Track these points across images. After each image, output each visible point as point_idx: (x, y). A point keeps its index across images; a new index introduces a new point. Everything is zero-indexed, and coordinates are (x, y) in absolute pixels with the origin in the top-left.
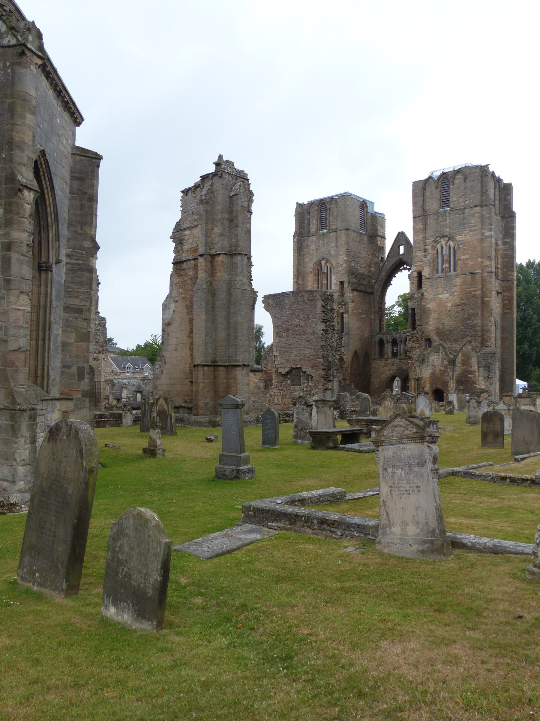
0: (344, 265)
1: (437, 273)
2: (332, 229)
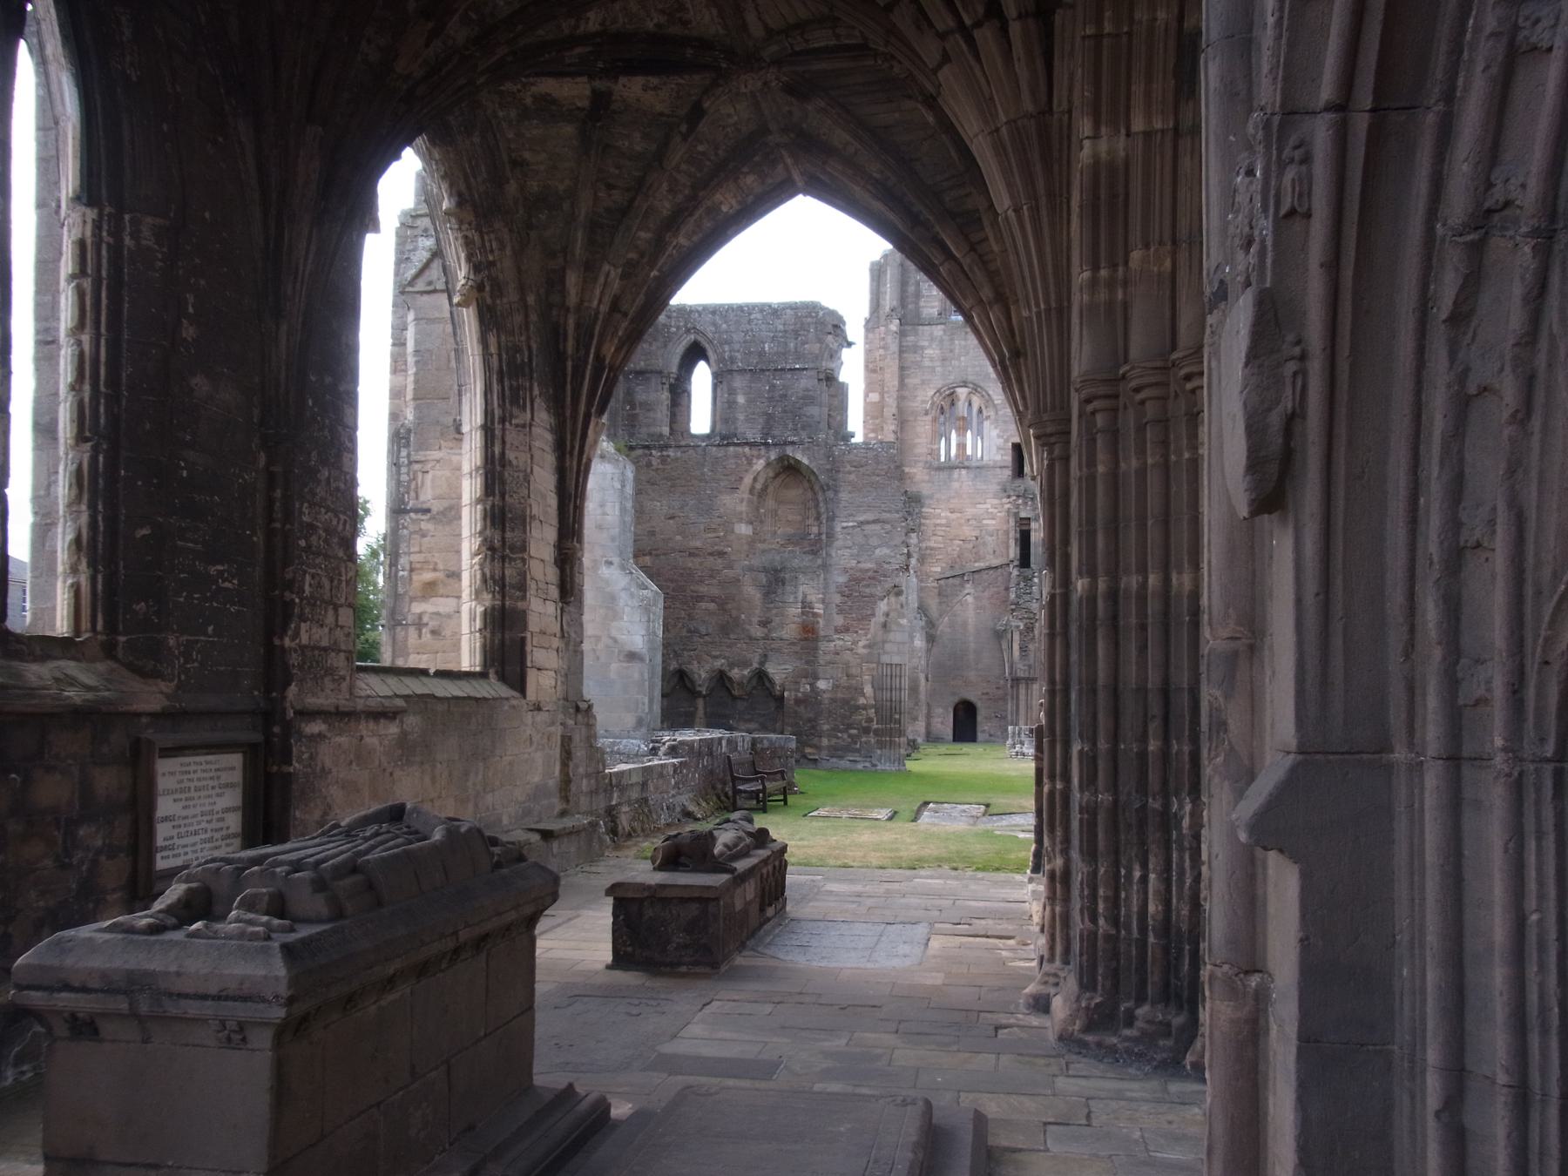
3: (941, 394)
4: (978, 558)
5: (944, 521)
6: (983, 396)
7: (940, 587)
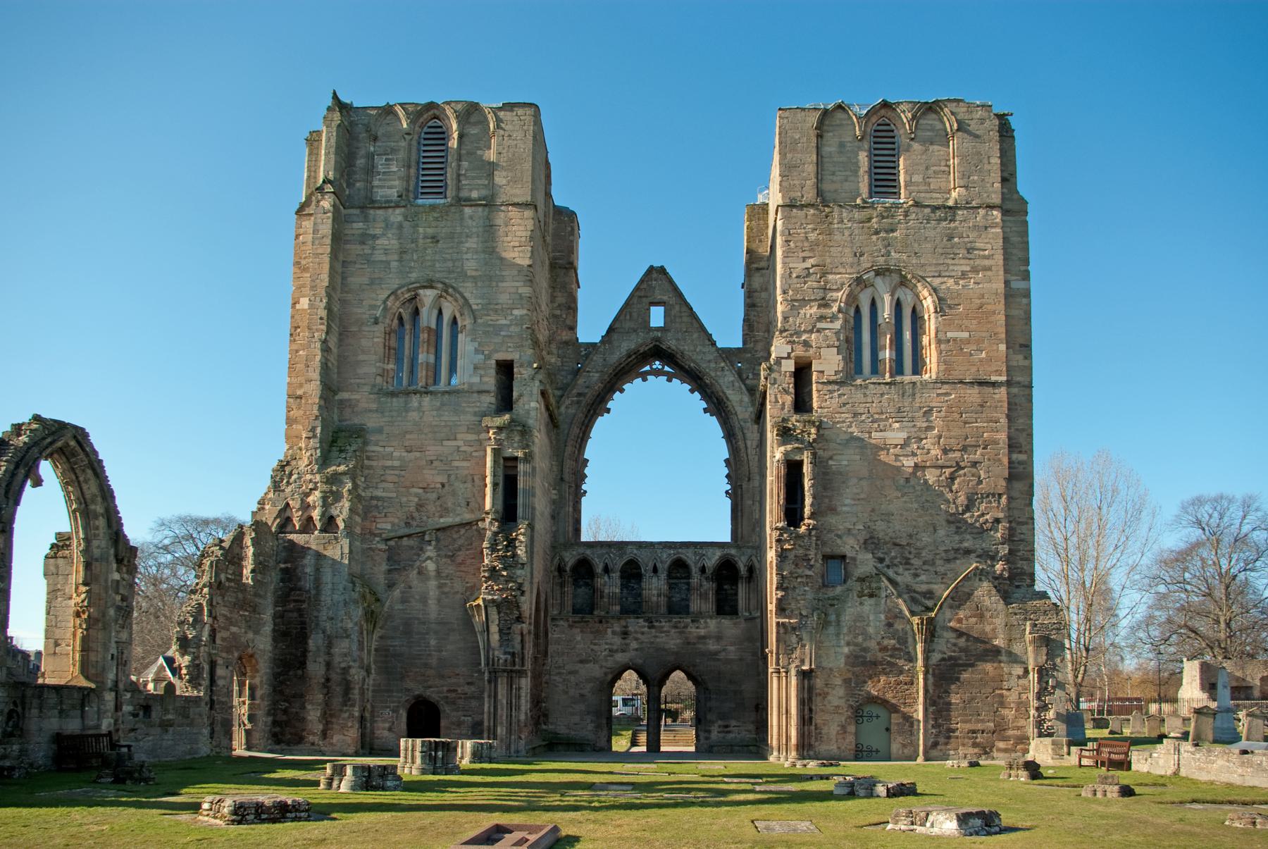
0: (516, 312)
2: (468, 199)
3: (397, 298)
4: (445, 511)
5: (396, 463)
7: (390, 548)
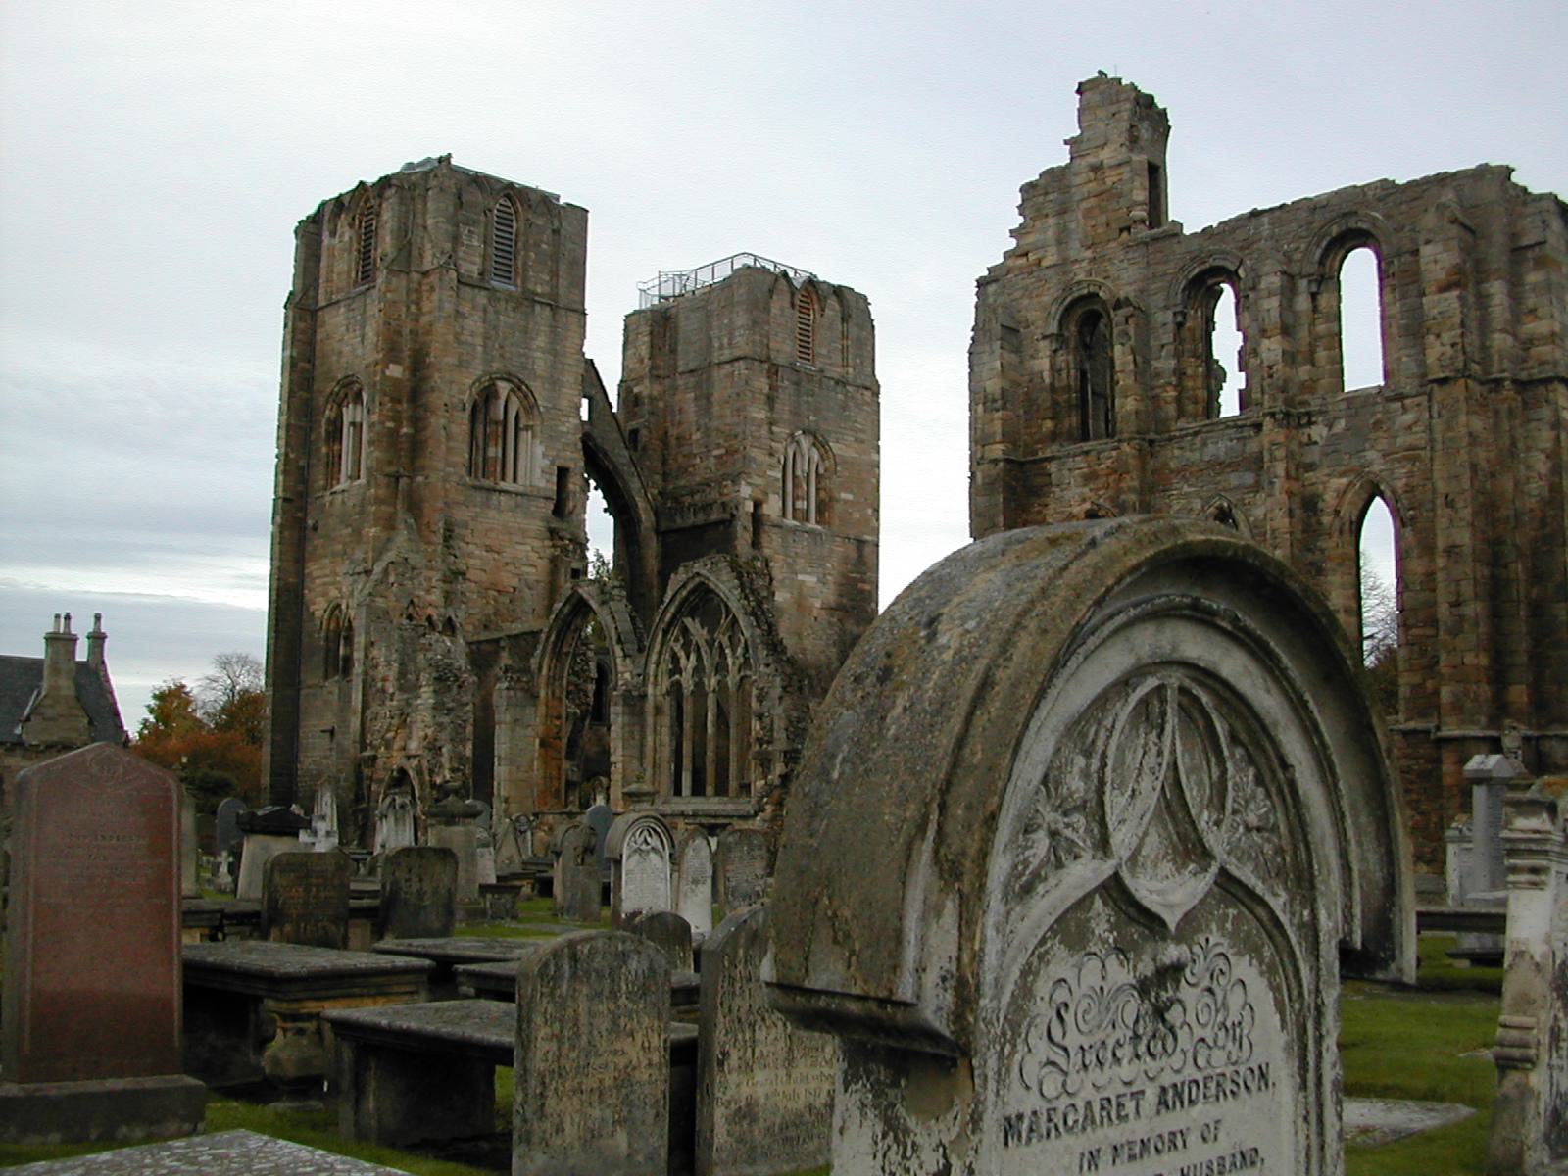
1: (784, 515)
6: (526, 396)
